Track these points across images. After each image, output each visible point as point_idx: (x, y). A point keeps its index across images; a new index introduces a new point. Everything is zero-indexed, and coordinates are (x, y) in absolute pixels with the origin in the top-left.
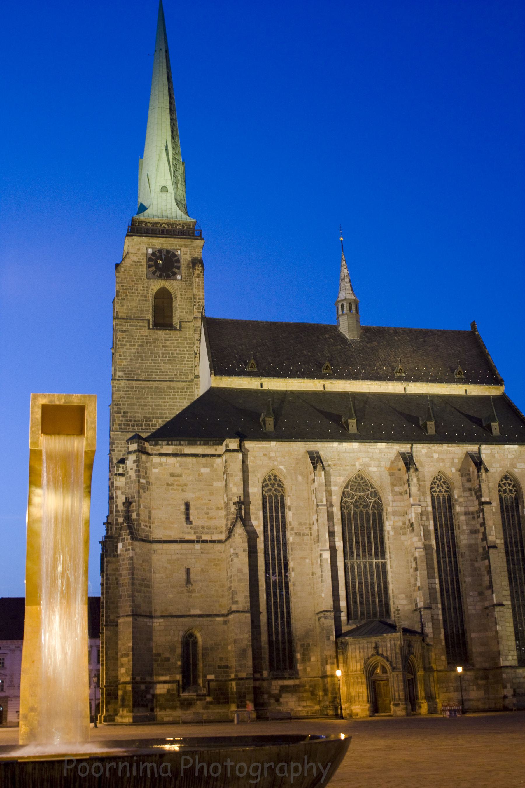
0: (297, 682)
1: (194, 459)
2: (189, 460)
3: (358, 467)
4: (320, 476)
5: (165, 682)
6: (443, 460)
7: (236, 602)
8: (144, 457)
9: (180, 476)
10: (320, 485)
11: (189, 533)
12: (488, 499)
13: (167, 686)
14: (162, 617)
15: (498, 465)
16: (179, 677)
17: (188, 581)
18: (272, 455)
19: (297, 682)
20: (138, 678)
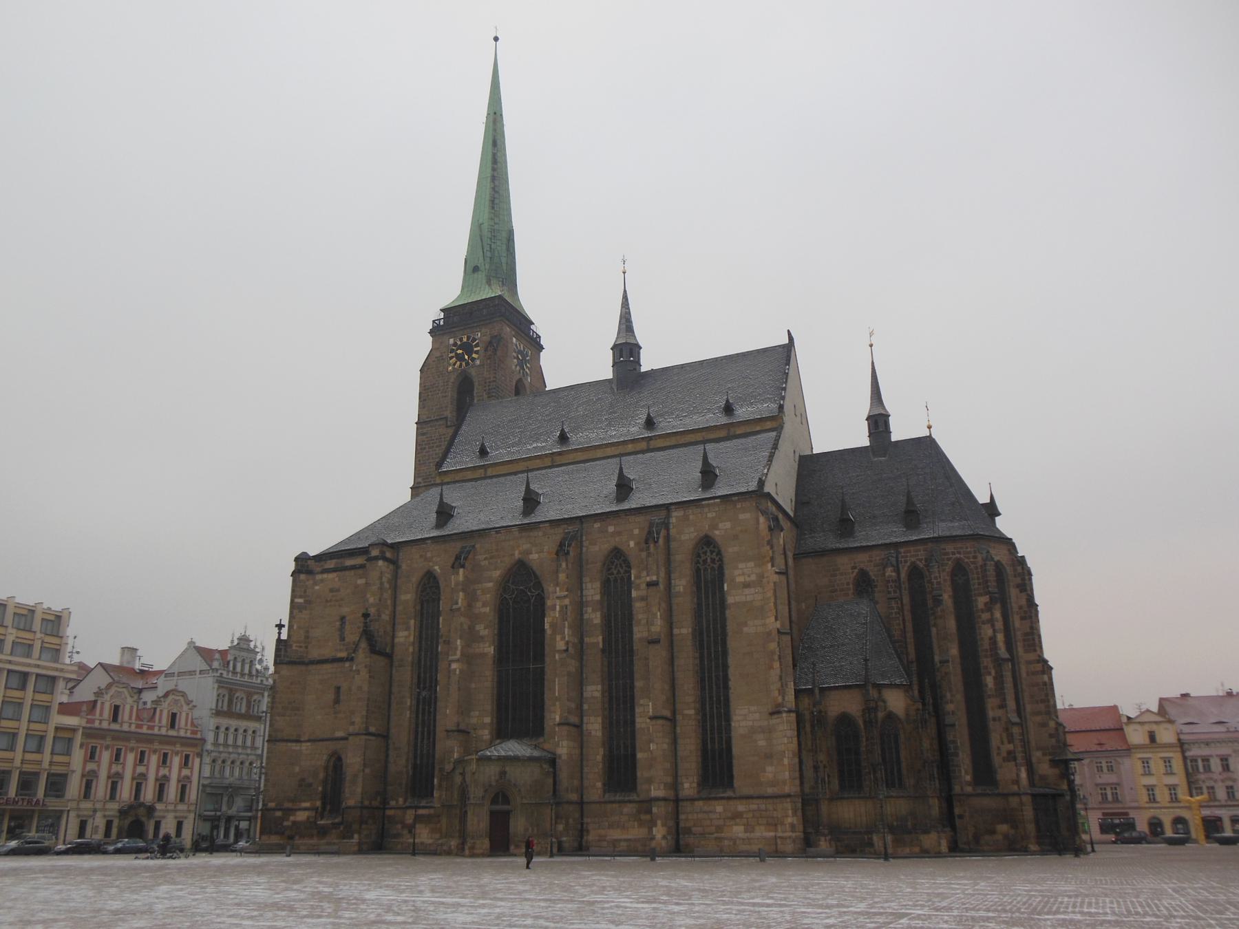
0: (432, 811)
1: (352, 573)
2: (347, 573)
3: (517, 555)
4: (458, 574)
5: (305, 809)
6: (619, 533)
7: (353, 723)
8: (303, 577)
9: (338, 590)
10: (457, 584)
11: (341, 650)
12: (654, 578)
13: (307, 813)
14: (309, 741)
15: (692, 529)
16: (318, 803)
17: (337, 701)
18: (429, 555)
19: (432, 811)
20: (272, 805)
